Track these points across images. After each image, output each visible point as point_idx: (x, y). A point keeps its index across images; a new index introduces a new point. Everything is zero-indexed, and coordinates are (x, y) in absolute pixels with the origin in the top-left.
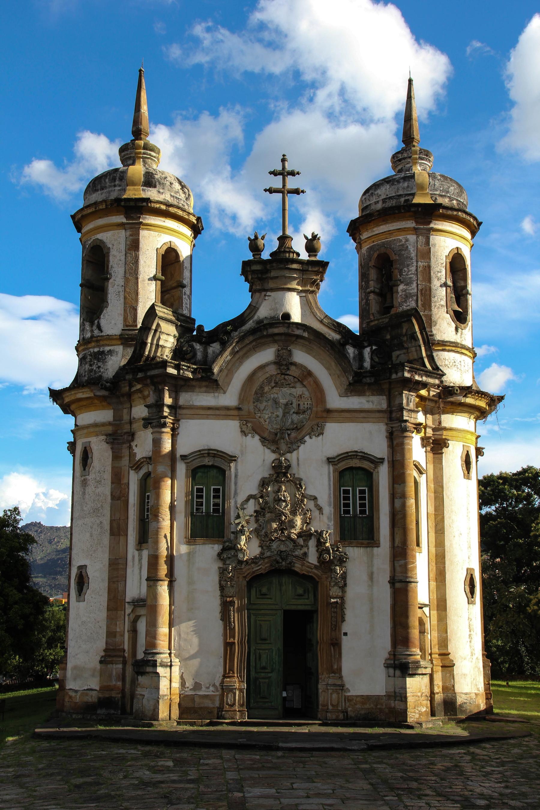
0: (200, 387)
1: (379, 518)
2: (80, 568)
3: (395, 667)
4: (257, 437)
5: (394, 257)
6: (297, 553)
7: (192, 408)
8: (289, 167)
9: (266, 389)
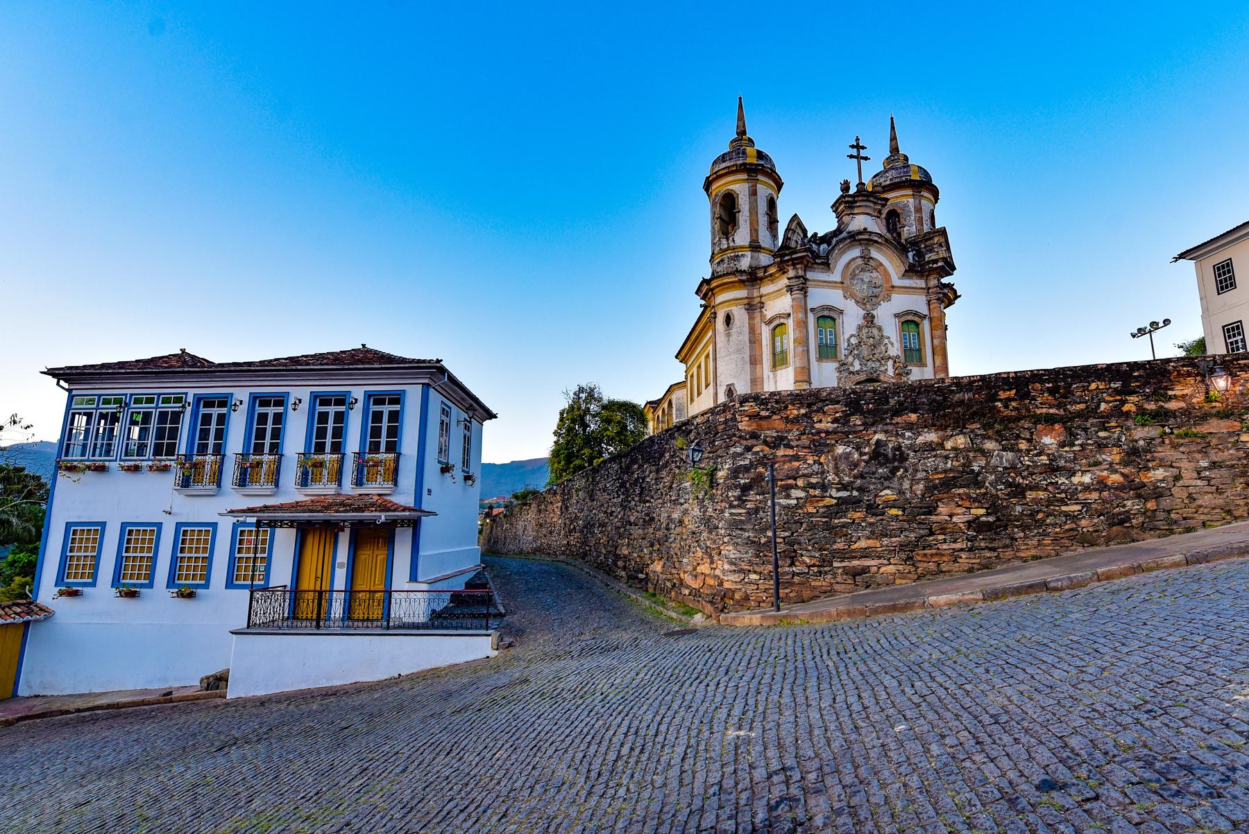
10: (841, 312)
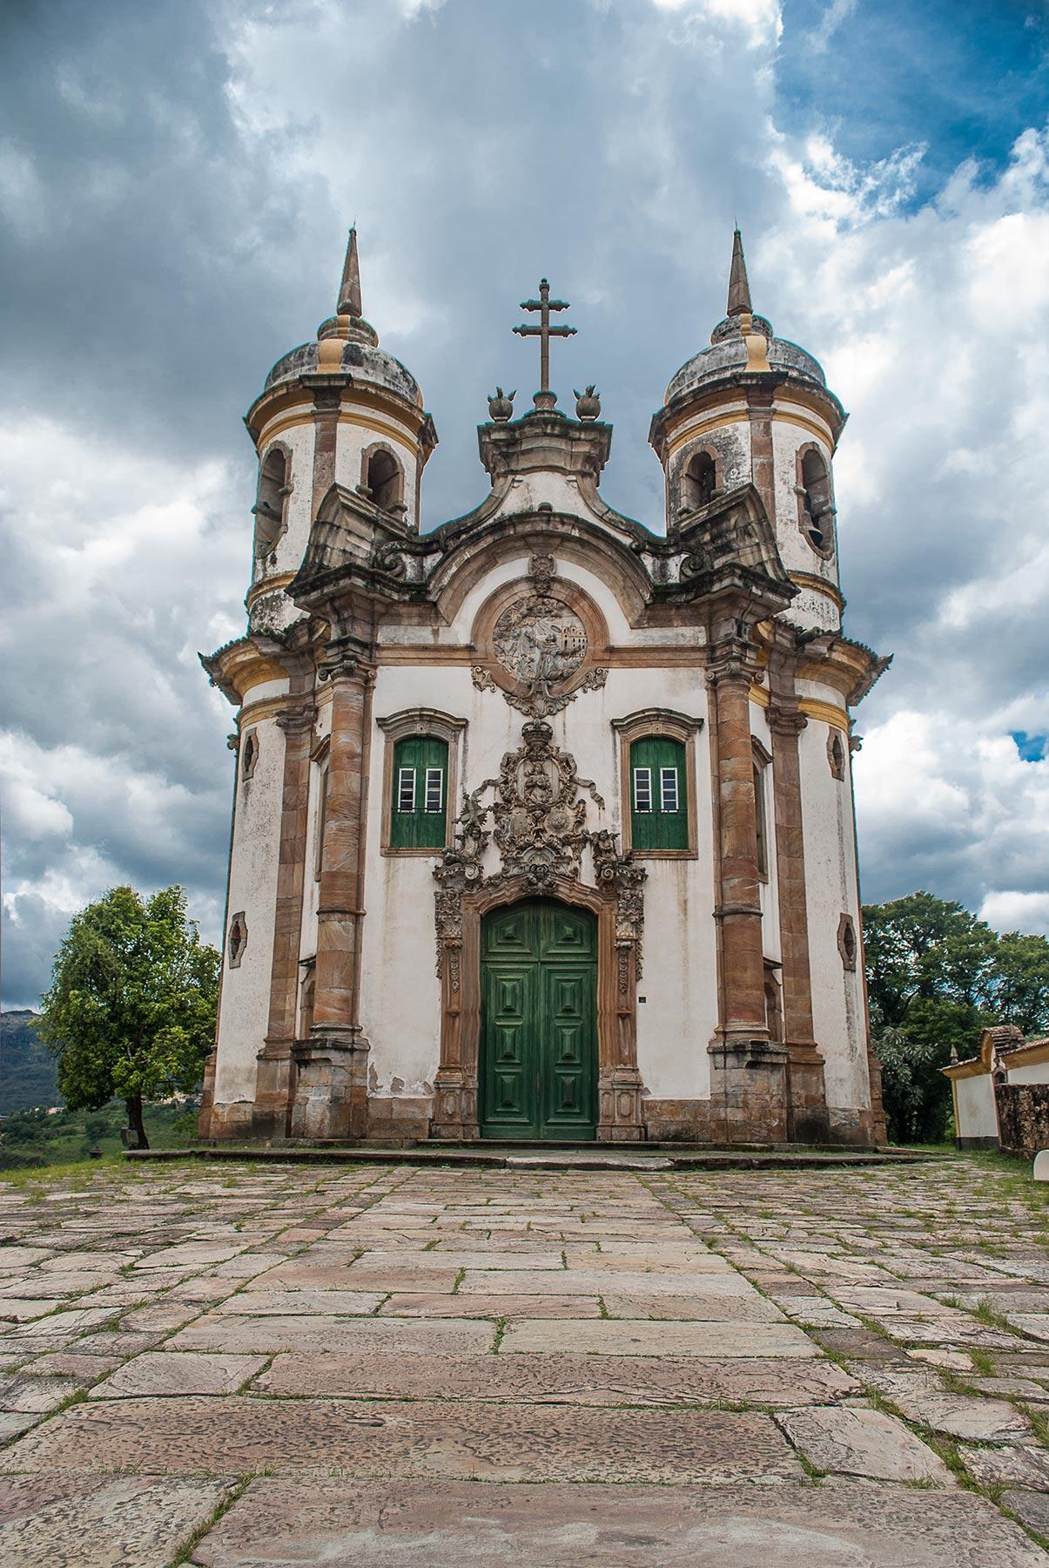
0: (410, 617)
1: (695, 815)
2: (236, 916)
3: (725, 1053)
4: (500, 692)
5: (716, 455)
6: (562, 870)
7: (396, 647)
8: (553, 297)
9: (514, 618)
10: (463, 725)
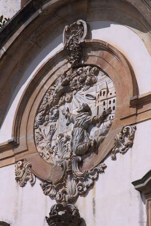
4: (38, 182)
